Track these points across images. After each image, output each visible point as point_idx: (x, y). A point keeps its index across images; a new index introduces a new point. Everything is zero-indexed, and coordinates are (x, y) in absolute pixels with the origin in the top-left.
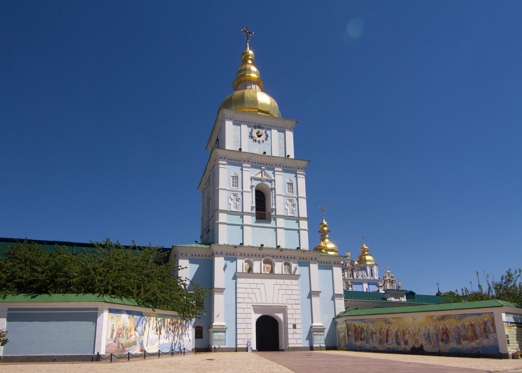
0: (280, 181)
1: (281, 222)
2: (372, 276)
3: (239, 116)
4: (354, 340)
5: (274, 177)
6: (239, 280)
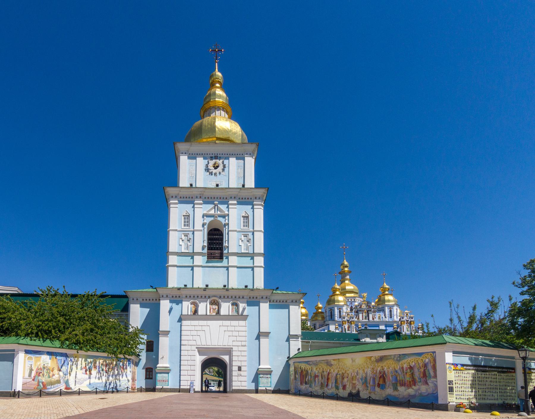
0: (235, 215)
1: (233, 261)
3: (194, 147)
4: (299, 383)
5: (228, 211)
6: (184, 323)
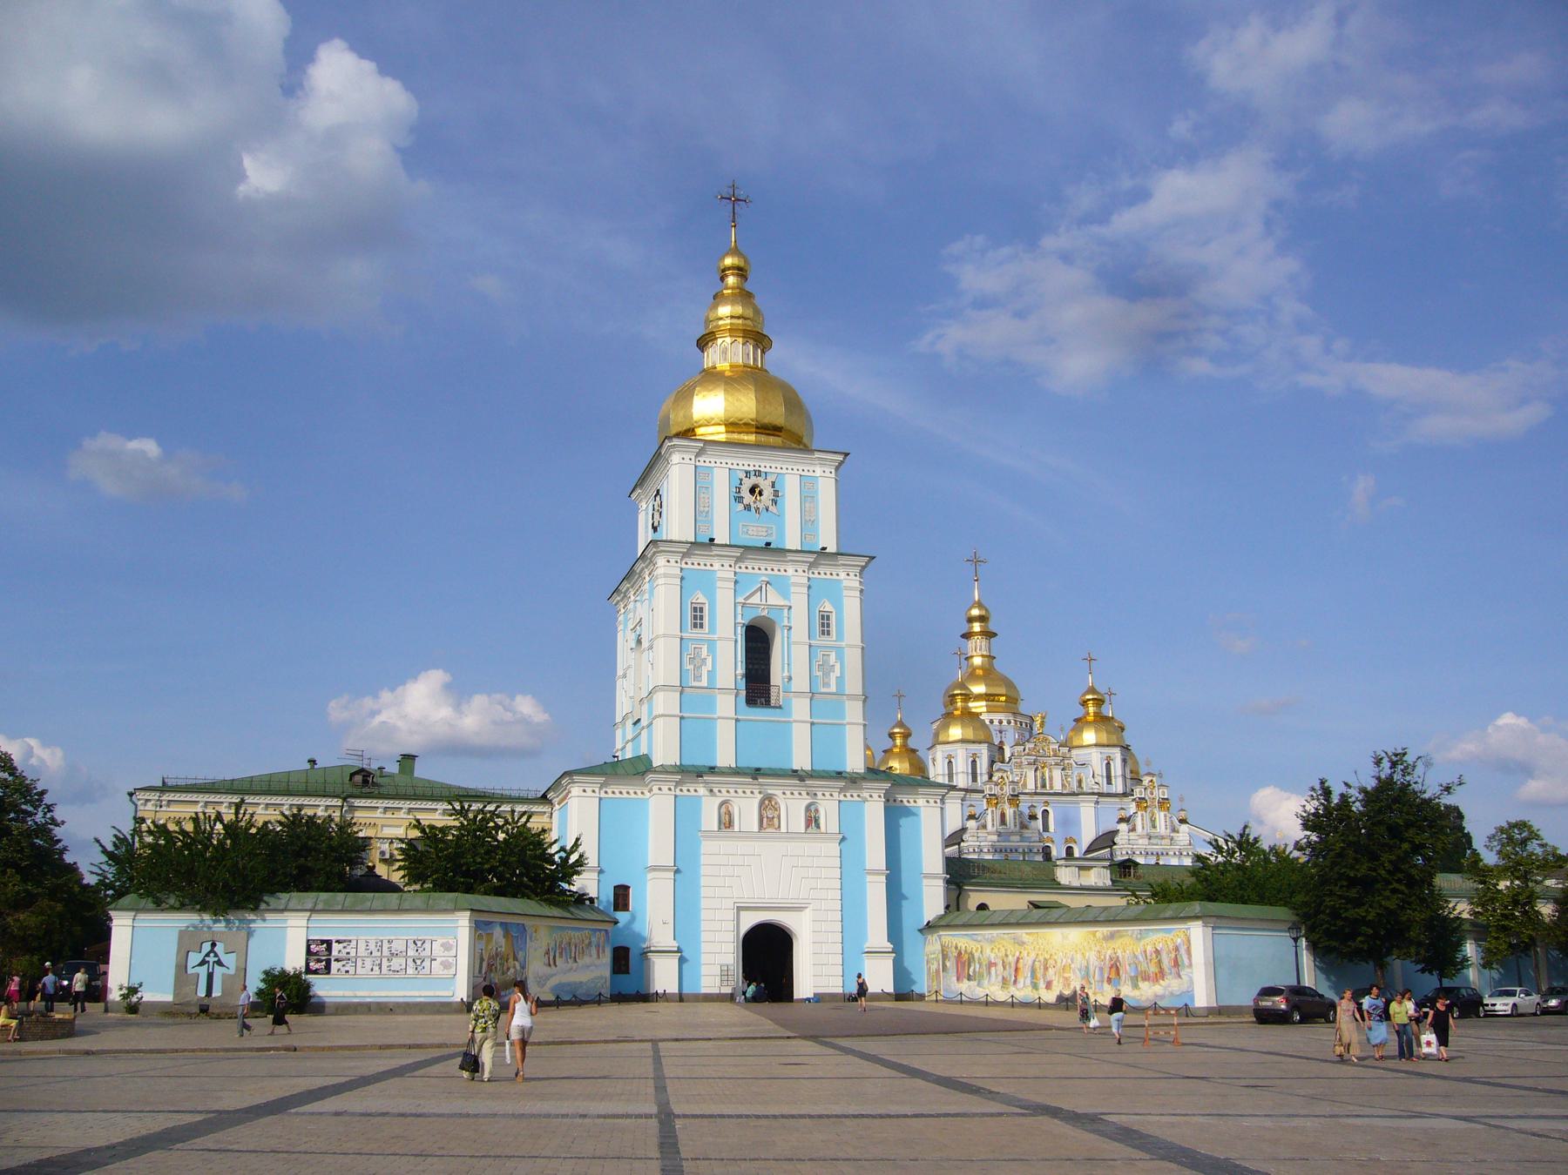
2: (1109, 782)
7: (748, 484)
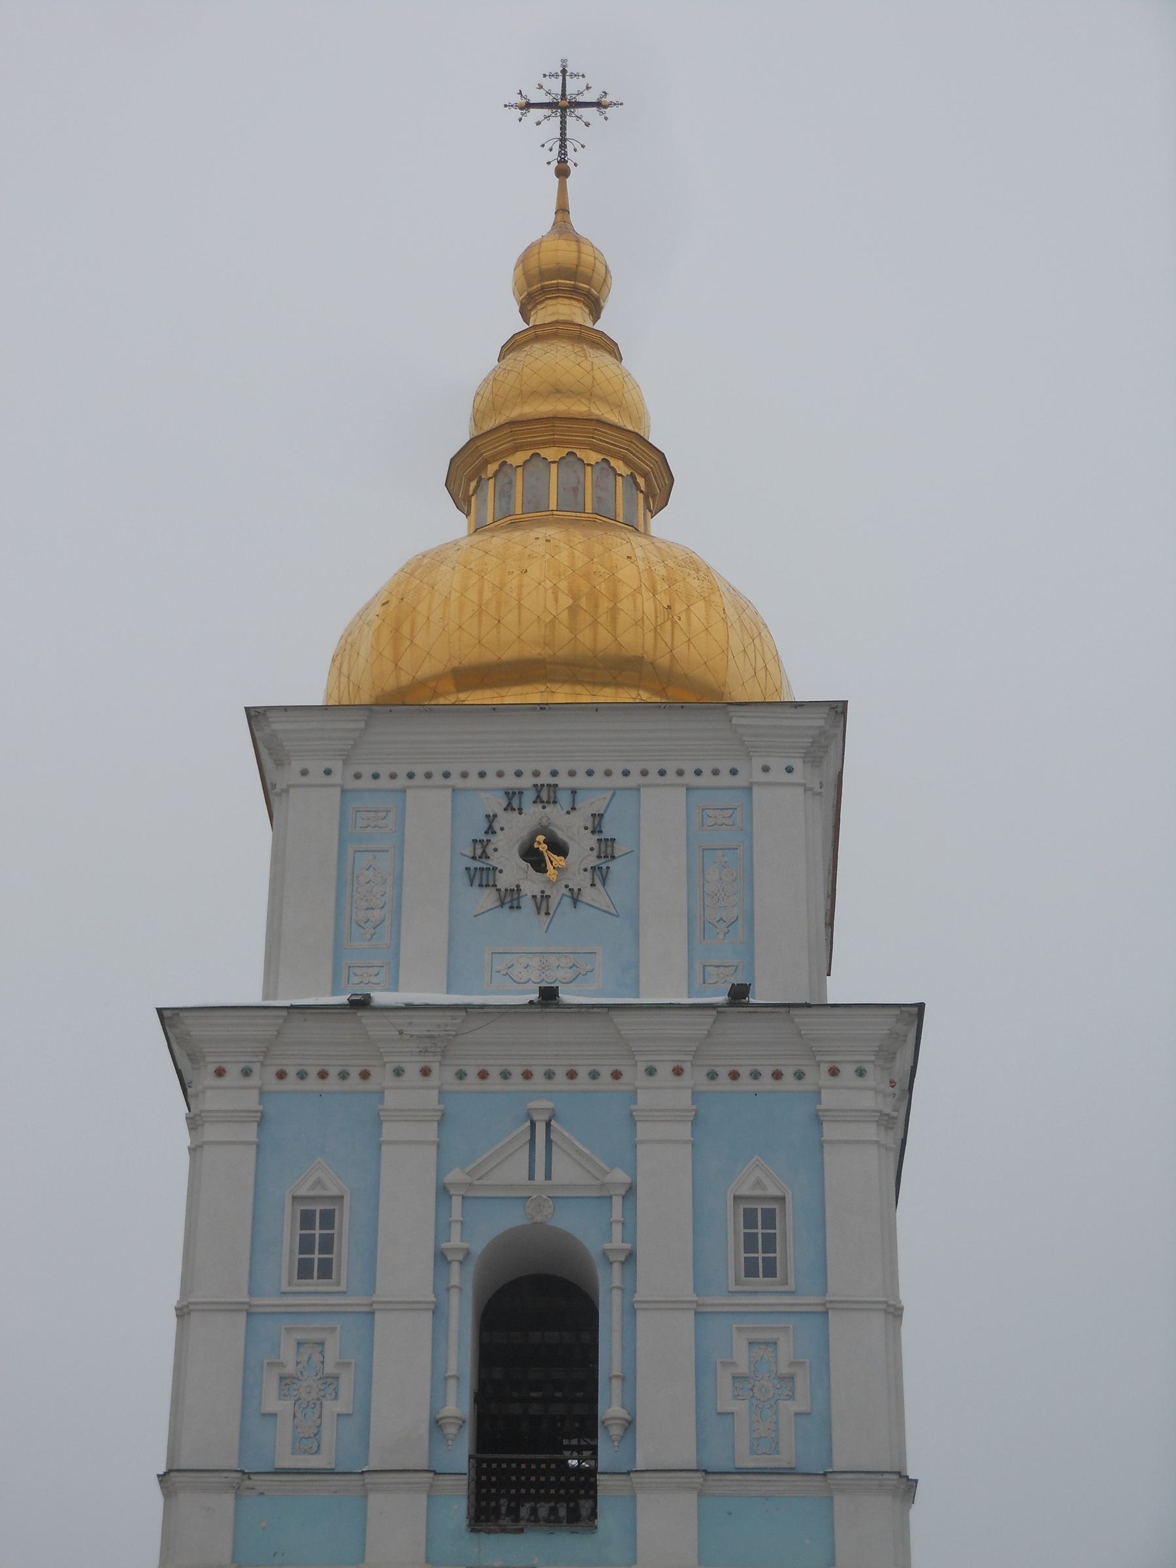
7: (515, 829)
